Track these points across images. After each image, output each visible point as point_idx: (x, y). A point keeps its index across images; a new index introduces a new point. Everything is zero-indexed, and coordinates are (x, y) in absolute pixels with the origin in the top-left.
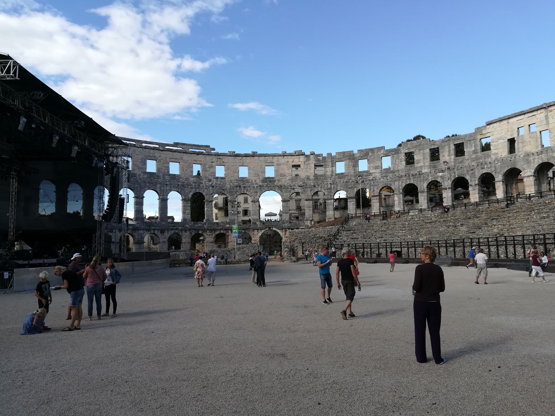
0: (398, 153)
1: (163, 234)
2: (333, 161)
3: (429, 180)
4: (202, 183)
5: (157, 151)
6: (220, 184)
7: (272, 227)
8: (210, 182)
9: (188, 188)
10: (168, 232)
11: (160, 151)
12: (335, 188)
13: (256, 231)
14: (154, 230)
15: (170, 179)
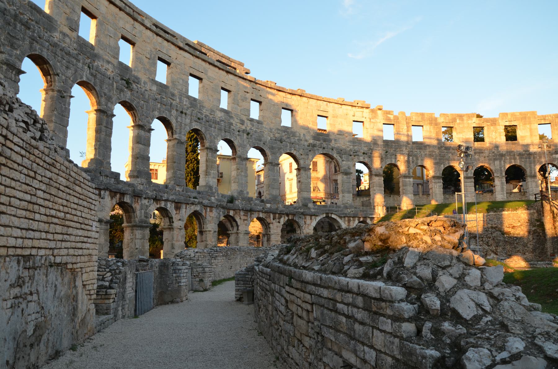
0: (495, 124)
1: (178, 212)
2: (409, 123)
3: (542, 162)
4: (232, 124)
5: (173, 46)
6: (256, 132)
7: (332, 214)
8: (243, 124)
9: (215, 128)
10: (186, 208)
11: (178, 49)
12: (415, 162)
13: (308, 218)
14: (167, 201)
15: (189, 106)
